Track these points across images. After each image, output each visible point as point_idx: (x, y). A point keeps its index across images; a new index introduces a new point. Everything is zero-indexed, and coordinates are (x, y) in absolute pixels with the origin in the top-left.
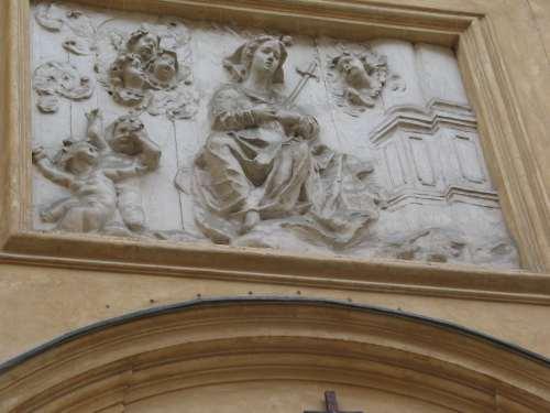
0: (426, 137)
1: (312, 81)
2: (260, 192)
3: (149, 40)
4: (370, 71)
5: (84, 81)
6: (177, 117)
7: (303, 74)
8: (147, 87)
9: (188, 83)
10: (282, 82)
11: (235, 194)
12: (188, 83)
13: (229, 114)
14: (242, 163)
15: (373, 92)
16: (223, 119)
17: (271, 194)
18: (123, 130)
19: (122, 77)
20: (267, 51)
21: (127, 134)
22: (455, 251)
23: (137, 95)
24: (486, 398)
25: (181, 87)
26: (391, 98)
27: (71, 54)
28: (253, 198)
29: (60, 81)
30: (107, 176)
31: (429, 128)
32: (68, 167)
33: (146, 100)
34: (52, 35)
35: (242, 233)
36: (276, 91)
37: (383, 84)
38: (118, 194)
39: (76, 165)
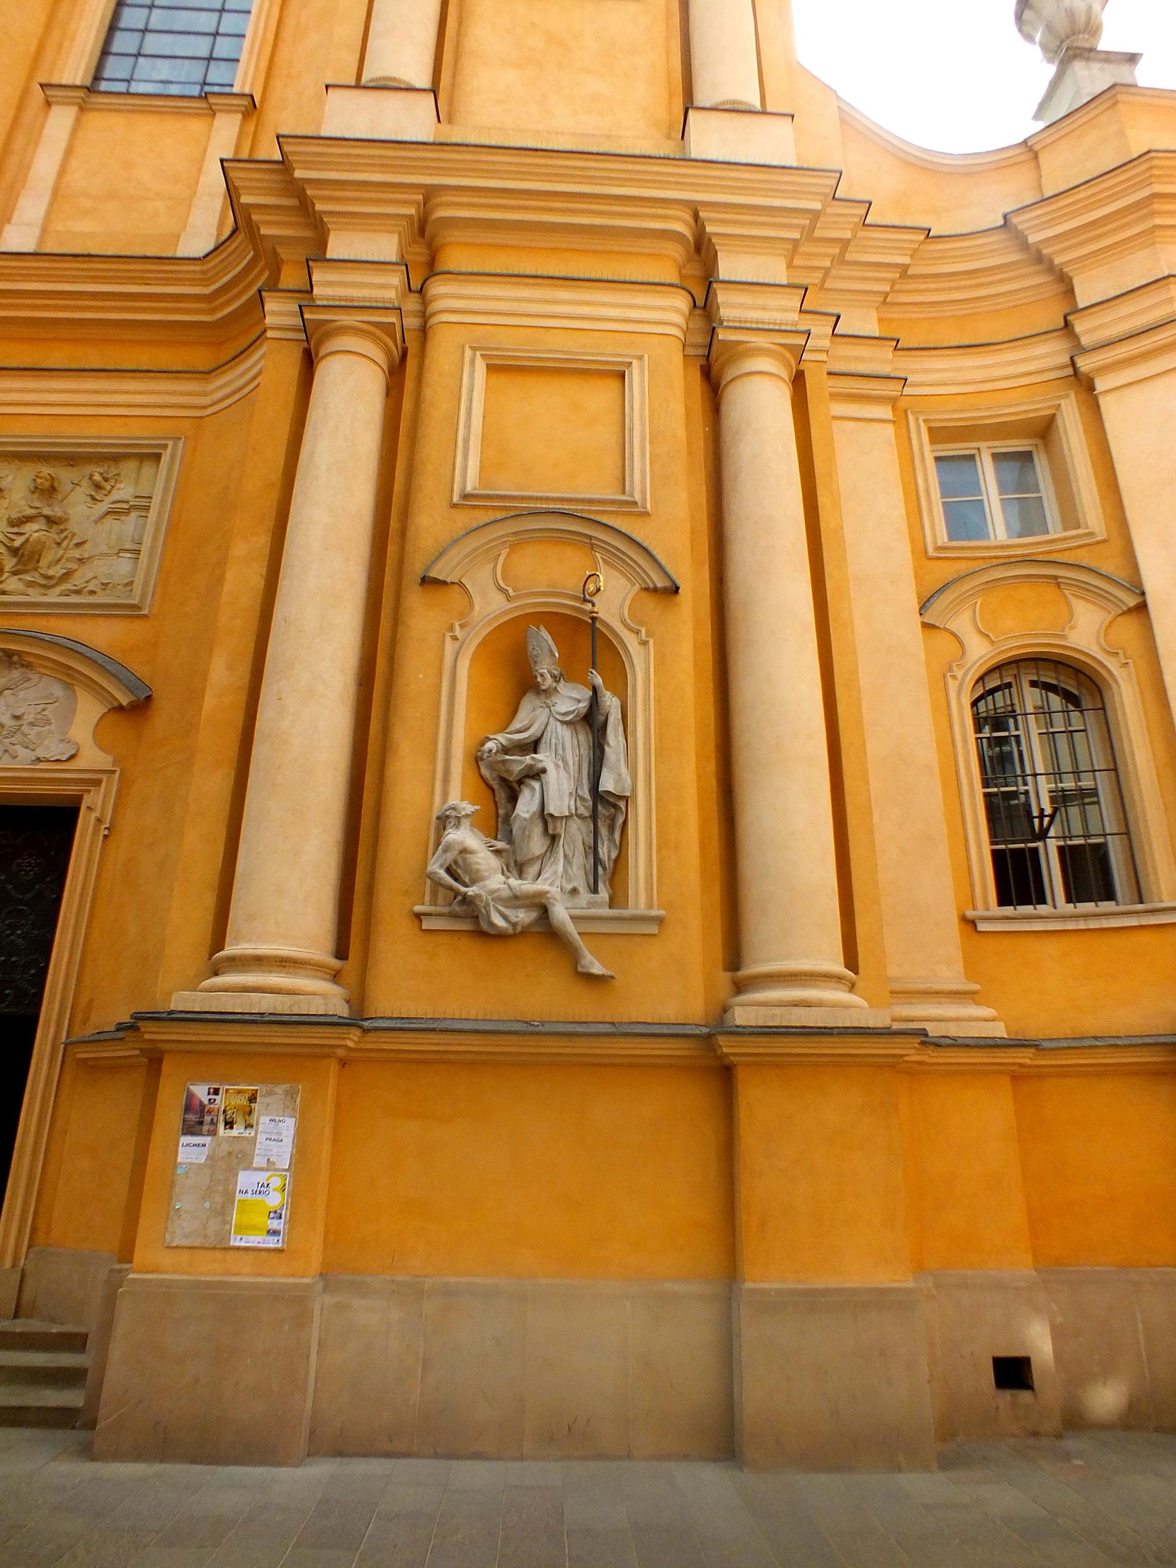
0: (123, 518)
2: (14, 561)
26: (115, 495)
31: (127, 512)
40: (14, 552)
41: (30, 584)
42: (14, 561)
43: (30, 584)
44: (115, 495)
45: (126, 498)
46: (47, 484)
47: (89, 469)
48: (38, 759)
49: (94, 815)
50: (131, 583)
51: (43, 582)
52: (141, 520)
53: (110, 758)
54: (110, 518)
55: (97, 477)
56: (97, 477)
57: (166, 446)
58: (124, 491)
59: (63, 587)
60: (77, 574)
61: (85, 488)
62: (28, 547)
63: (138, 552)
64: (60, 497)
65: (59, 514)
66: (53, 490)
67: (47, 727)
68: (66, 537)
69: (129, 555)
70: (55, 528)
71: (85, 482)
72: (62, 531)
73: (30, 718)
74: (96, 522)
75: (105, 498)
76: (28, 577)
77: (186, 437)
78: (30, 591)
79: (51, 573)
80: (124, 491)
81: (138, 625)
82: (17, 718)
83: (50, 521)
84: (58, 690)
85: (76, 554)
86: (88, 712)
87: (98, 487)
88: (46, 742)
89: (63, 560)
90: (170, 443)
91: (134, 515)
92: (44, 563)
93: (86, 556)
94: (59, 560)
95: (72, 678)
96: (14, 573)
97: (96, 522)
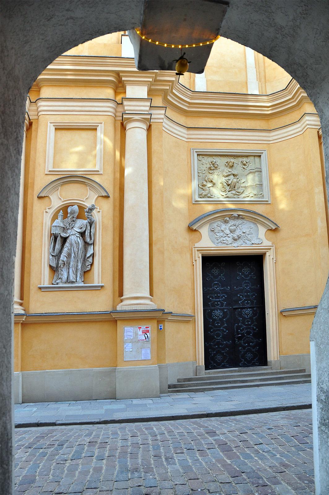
4: (247, 163)
5: (205, 170)
8: (214, 170)
14: (227, 184)
24: (255, 220)
39: (204, 186)
40: (228, 185)
41: (235, 195)
43: (235, 195)
47: (240, 159)
48: (253, 244)
49: (271, 257)
50: (262, 194)
51: (238, 194)
52: (259, 175)
53: (271, 243)
55: (245, 162)
56: (245, 162)
62: (233, 183)
63: (262, 185)
66: (233, 166)
67: (252, 235)
68: (239, 180)
71: (239, 163)
72: (238, 178)
73: (248, 233)
76: (234, 192)
78: (235, 196)
79: (239, 191)
81: (268, 206)
82: (244, 233)
84: (252, 226)
86: (262, 230)
88: (253, 239)
89: (240, 187)
95: (257, 221)
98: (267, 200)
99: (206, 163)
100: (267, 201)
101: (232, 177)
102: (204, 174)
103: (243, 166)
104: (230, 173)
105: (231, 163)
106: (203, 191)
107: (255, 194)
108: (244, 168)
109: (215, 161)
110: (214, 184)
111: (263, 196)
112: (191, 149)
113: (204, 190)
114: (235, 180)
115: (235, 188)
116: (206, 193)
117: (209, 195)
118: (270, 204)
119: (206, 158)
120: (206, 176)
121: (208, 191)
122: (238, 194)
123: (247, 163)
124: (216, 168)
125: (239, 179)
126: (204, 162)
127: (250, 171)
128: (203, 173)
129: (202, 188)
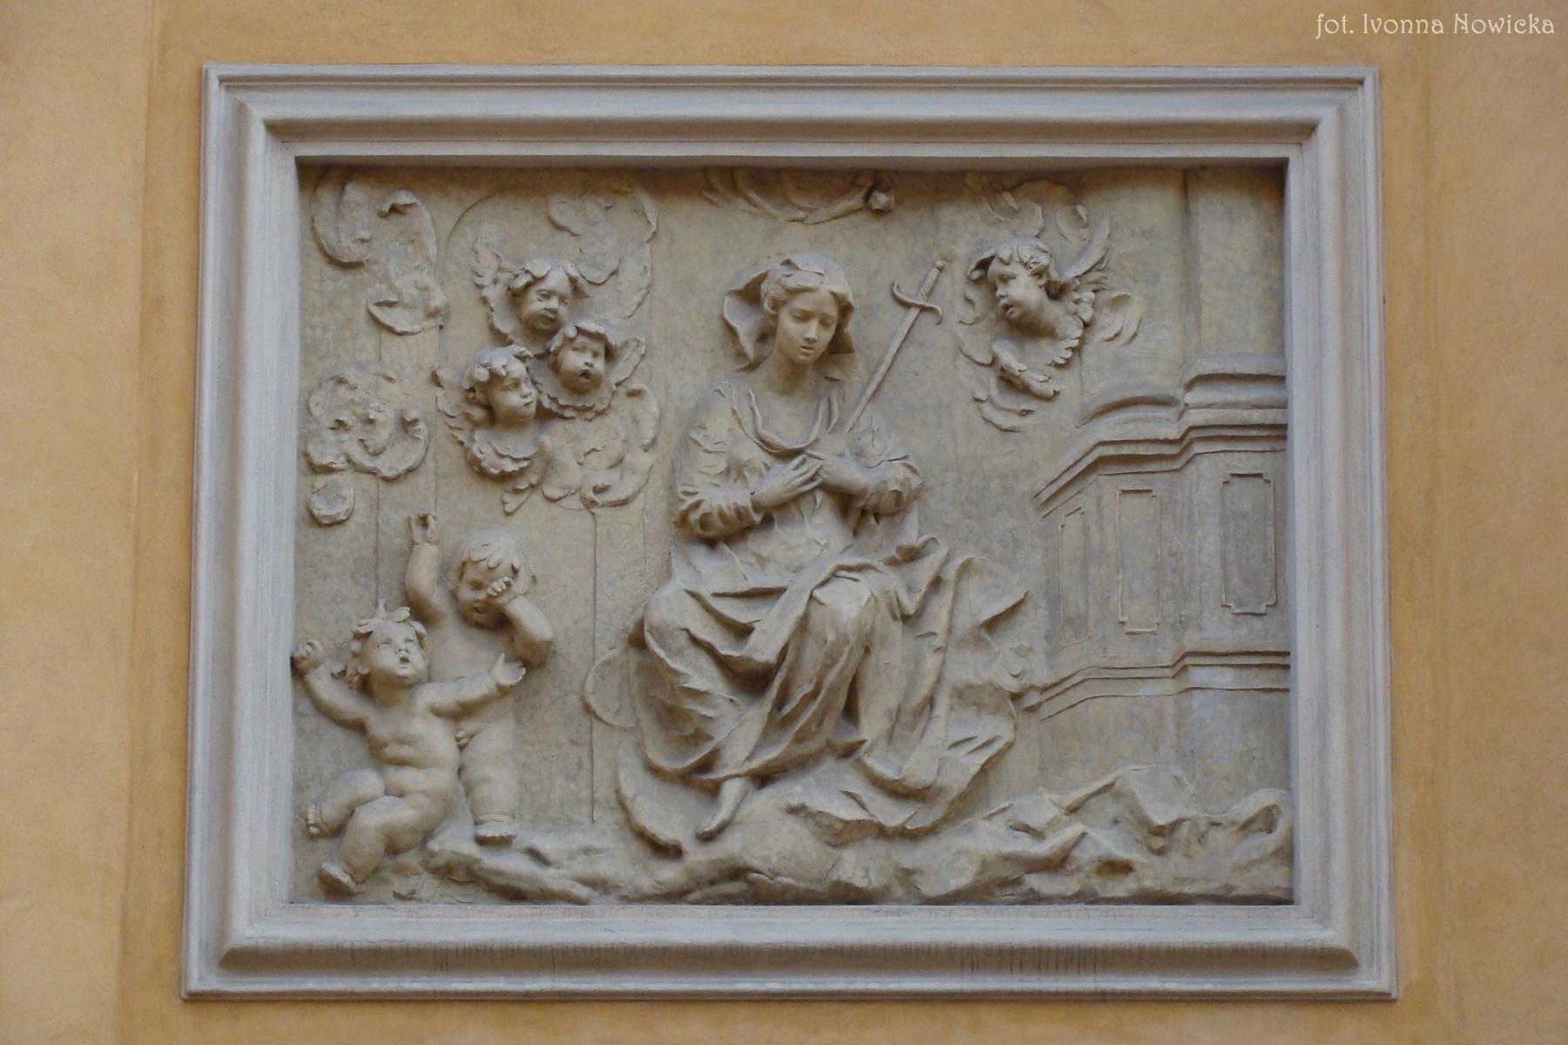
0: (1159, 484)
1: (928, 318)
2: (756, 715)
3: (547, 295)
4: (1056, 292)
5: (406, 426)
6: (599, 499)
7: (907, 305)
8: (544, 415)
9: (634, 394)
10: (850, 351)
11: (699, 737)
12: (634, 394)
13: (704, 508)
14: (722, 662)
15: (1061, 353)
16: (694, 517)
17: (778, 722)
18: (477, 586)
19: (489, 408)
20: (805, 317)
21: (482, 596)
22: (1158, 842)
23: (516, 460)
25: (625, 405)
27: (385, 336)
28: (740, 731)
29: (358, 431)
30: (438, 713)
32: (366, 686)
33: (538, 463)
34: (344, 280)
35: (707, 838)
36: (837, 374)
37: (1086, 325)
38: (461, 748)
39: (375, 686)
40: (751, 680)
41: (840, 835)
42: (756, 715)
44: (1099, 377)
45: (1160, 382)
46: (827, 335)
50: (1267, 820)
51: (893, 815)
52: (1246, 497)
54: (1108, 485)
56: (1024, 291)
57: (1306, 130)
58: (1140, 347)
59: (987, 838)
60: (1020, 765)
61: (957, 343)
62: (812, 656)
63: (1279, 660)
64: (857, 373)
65: (895, 477)
66: (839, 347)
68: (937, 583)
69: (1226, 678)
70: (882, 541)
71: (953, 293)
72: (912, 556)
74: (1047, 503)
75: (1065, 383)
76: (830, 793)
77: (1380, 79)
79: (917, 767)
80: (1140, 347)
81: (1349, 1030)
83: (854, 509)
85: (1001, 667)
87: (1025, 328)
89: (941, 709)
90: (1322, 109)
91: (1209, 470)
92: (872, 725)
93: (1042, 676)
94: (931, 701)
96: (763, 778)
97: (1047, 503)
98: (1331, 936)
99: (438, 300)
100: (1335, 960)
101: (817, 536)
102: (396, 490)
103: (1009, 357)
104: (779, 480)
105: (805, 317)
106: (369, 781)
107: (1159, 831)
108: (1011, 383)
109: (556, 281)
110: (535, 660)
111: (1287, 854)
112: (202, 79)
113: (378, 755)
114: (849, 603)
115: (851, 712)
116: (402, 814)
117: (455, 842)
118: (1383, 999)
119: (430, 216)
120: (424, 522)
121: (440, 779)
122: (893, 815)
123: (1056, 292)
124: (581, 384)
125: (924, 571)
126: (405, 284)
127: (1107, 428)
128: (386, 465)
129: (359, 727)
